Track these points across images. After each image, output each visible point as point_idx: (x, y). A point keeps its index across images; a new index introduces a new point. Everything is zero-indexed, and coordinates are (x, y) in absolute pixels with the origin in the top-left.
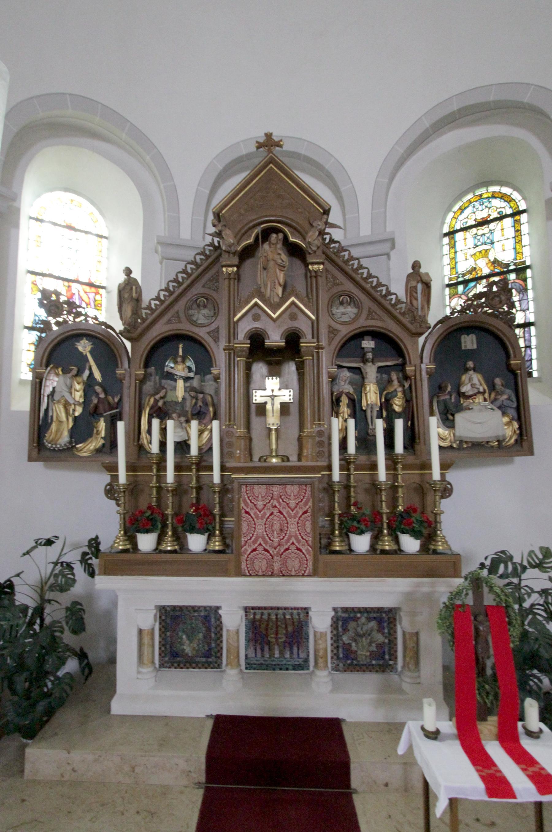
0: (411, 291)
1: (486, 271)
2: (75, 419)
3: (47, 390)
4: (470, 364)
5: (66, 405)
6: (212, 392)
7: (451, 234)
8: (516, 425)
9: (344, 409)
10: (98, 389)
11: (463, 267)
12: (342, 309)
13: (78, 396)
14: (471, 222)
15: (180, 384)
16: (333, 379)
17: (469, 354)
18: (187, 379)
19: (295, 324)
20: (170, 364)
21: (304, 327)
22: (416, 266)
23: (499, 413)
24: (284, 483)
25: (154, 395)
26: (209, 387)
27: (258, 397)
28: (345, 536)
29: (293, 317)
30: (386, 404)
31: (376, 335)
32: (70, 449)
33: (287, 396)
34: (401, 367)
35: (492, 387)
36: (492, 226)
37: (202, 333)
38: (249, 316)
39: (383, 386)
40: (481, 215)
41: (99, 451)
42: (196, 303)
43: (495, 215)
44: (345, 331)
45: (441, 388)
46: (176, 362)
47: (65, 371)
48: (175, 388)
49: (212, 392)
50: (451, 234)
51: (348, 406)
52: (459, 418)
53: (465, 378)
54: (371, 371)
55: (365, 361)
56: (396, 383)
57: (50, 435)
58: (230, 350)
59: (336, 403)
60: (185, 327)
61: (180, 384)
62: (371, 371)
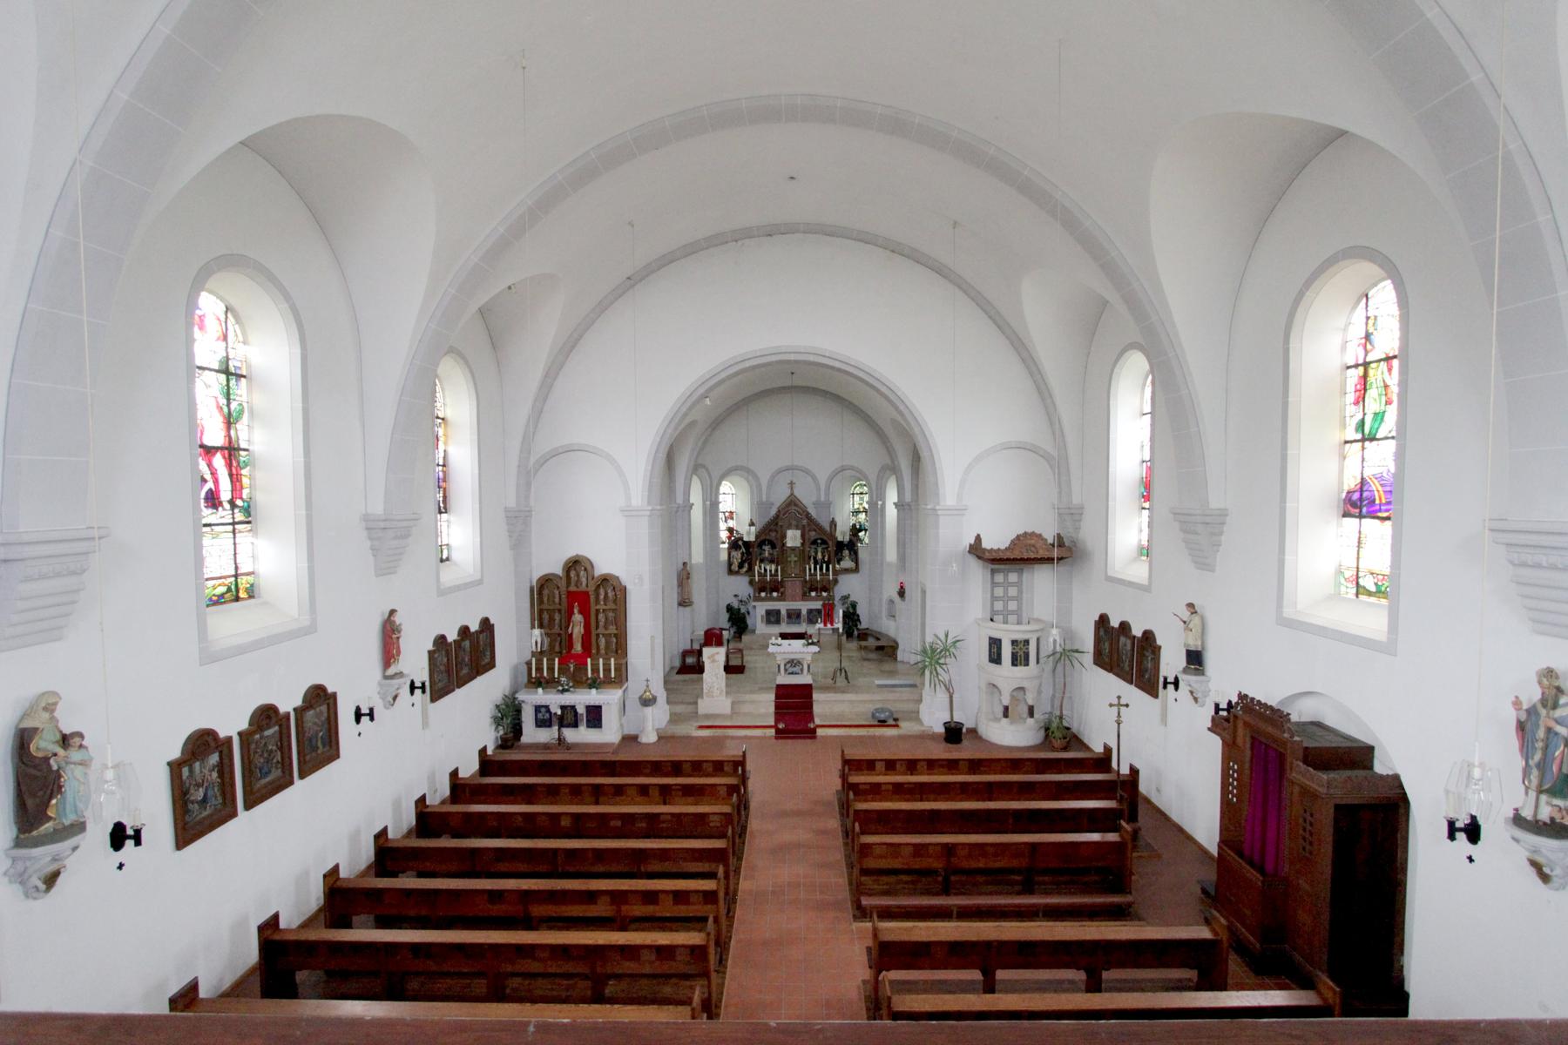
0: (831, 527)
1: (862, 510)
7: (853, 494)
11: (856, 506)
15: (767, 552)
20: (764, 547)
28: (809, 592)
30: (823, 558)
31: (821, 539)
33: (796, 559)
34: (827, 548)
37: (773, 539)
40: (861, 491)
41: (746, 571)
42: (770, 530)
44: (812, 539)
50: (853, 494)
52: (841, 563)
54: (820, 549)
57: (733, 567)
59: (810, 558)
60: (768, 537)
61: (767, 552)
62: (820, 549)
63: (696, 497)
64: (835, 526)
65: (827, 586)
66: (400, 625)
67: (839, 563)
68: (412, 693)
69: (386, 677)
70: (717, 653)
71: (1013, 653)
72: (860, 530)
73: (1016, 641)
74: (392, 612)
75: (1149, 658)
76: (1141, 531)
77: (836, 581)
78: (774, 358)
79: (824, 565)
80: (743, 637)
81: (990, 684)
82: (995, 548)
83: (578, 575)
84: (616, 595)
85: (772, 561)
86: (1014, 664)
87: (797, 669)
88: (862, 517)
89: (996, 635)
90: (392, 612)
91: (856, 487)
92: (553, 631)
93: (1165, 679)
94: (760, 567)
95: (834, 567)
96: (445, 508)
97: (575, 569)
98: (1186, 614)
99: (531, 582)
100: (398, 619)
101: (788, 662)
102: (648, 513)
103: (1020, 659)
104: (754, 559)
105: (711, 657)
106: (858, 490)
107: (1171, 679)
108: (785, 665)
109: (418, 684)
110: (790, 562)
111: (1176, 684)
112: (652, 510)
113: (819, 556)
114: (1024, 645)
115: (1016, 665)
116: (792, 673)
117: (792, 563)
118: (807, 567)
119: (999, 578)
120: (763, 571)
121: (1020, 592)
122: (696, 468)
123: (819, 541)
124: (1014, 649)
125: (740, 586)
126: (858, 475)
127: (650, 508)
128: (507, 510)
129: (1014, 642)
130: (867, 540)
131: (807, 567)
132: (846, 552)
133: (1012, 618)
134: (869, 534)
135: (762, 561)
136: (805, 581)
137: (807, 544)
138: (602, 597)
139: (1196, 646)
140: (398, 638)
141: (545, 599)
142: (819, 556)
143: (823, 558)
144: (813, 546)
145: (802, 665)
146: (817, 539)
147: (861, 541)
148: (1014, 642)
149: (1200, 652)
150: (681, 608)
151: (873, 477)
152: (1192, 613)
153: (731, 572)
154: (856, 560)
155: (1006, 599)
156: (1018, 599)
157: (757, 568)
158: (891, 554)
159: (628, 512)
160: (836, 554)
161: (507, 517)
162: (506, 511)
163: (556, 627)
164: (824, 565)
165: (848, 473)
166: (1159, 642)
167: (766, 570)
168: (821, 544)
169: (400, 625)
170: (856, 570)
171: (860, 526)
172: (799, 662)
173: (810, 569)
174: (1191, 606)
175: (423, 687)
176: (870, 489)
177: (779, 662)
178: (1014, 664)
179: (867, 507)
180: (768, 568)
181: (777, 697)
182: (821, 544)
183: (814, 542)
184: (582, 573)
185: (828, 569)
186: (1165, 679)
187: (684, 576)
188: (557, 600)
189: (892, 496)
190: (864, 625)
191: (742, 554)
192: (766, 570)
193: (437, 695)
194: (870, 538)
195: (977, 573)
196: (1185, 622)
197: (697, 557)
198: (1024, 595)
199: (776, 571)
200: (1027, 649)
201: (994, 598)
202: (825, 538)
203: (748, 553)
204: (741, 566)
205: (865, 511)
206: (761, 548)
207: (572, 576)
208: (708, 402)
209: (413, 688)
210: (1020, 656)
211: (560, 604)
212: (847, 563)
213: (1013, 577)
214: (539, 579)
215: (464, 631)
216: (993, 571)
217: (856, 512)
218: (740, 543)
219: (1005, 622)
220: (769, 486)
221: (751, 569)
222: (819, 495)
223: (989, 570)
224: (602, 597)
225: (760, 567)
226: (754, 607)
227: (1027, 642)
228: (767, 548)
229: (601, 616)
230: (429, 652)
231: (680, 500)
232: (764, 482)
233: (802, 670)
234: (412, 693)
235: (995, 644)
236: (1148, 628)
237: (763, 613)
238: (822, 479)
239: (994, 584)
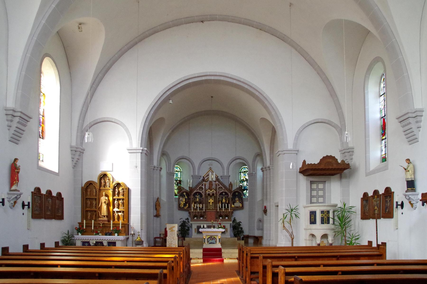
0: (229, 186)
1: (245, 180)
2: (184, 203)
3: (180, 200)
4: (237, 197)
5: (183, 201)
6: (202, 200)
7: (241, 173)
8: (242, 205)
9: (220, 202)
10: (187, 199)
11: (242, 178)
12: (220, 189)
13: (184, 200)
14: (243, 171)
15: (198, 199)
16: (219, 198)
17: (237, 195)
18: (199, 198)
19: (214, 193)
21: (214, 193)
22: (231, 182)
23: (240, 203)
24: (212, 211)
25: (194, 200)
26: (202, 199)
27: (209, 201)
29: (213, 192)
30: (226, 202)
31: (225, 192)
32: (183, 208)
33: (213, 201)
34: (228, 197)
35: (239, 200)
36: (246, 173)
38: (208, 192)
39: (225, 199)
40: (245, 170)
43: (246, 171)
45: (233, 200)
46: (197, 196)
47: (182, 197)
48: (197, 199)
49: (202, 200)
51: (221, 202)
52: (235, 204)
53: (236, 198)
54: (224, 197)
55: (223, 196)
56: (227, 199)
58: (205, 194)
59: (219, 202)
61: (198, 199)
62: (224, 197)
63: (164, 165)
64: (232, 186)
65: (228, 214)
66: (19, 166)
67: (234, 204)
68: (23, 208)
69: (11, 191)
70: (174, 227)
71: (322, 217)
72: (244, 190)
74: (16, 160)
75: (388, 201)
76: (382, 151)
77: (232, 213)
78: (204, 78)
79: (226, 205)
80: (186, 238)
81: (311, 234)
82: (313, 163)
83: (105, 182)
84: (124, 192)
85: (200, 203)
86: (322, 222)
87: (213, 241)
88: (245, 183)
89: (313, 209)
90: (16, 160)
91: (242, 169)
92: (92, 209)
93: (397, 202)
94: (194, 206)
95: (231, 206)
96: (42, 136)
97: (104, 179)
98: (405, 165)
99: (82, 185)
100: (18, 163)
101: (209, 238)
102: (141, 151)
103: (325, 220)
104: (191, 203)
105: (171, 229)
106: (243, 170)
107: (400, 203)
108: (208, 239)
109: (26, 203)
110: (210, 202)
111: (402, 205)
112: (142, 150)
113: (224, 201)
114: (327, 214)
115: (323, 223)
116: (210, 243)
117: (211, 204)
118: (218, 204)
119: (314, 186)
120: (196, 208)
121: (324, 193)
122: (164, 154)
123: (224, 193)
124: (322, 215)
125: (184, 215)
126: (241, 161)
127: (142, 148)
128: (71, 147)
129: (322, 212)
130: (247, 195)
131: (218, 204)
132: (237, 199)
133: (321, 200)
134: (248, 191)
135: (195, 203)
136: (218, 212)
137: (218, 194)
138: (116, 193)
139: (412, 178)
140: (18, 172)
141: (89, 193)
142: (224, 201)
143: (226, 202)
144: (221, 196)
145: (216, 239)
146: (223, 192)
147: (244, 195)
148: (322, 212)
149: (413, 180)
150: (155, 218)
151: (250, 162)
152: (409, 163)
153: (180, 208)
154: (242, 203)
155: (318, 197)
156: (323, 196)
157: (193, 205)
158: (259, 197)
159: (131, 151)
160: (232, 200)
161: (71, 150)
162: (71, 147)
163: (94, 207)
164: (226, 205)
165: (238, 161)
166: (392, 191)
167: (197, 207)
168: (225, 195)
169: (19, 166)
170: (242, 208)
171: (244, 188)
172: (215, 238)
173: (219, 207)
174: (408, 160)
175: (28, 205)
176: (249, 168)
177: (204, 237)
178: (322, 222)
179: (247, 178)
180: (198, 206)
181: (203, 251)
182: (225, 195)
183: (221, 194)
184: (107, 181)
185: (228, 207)
186: (397, 202)
187: (157, 205)
188: (94, 194)
189: (259, 167)
190: (246, 233)
191: (186, 199)
192: (197, 207)
193: (35, 216)
194: (249, 193)
195: (303, 181)
196: (405, 169)
197: (164, 198)
198: (327, 194)
199: (203, 207)
200: (329, 215)
201: (312, 197)
202: (226, 191)
203: (189, 199)
204: (185, 205)
205: (247, 180)
206: (195, 196)
207: (103, 182)
208: (171, 102)
209: (23, 205)
210: (325, 219)
211: (96, 196)
212: (238, 204)
213: (321, 186)
214: (86, 183)
215: (49, 192)
216: (312, 183)
217: (243, 181)
218: (185, 194)
219: (318, 202)
220: (199, 168)
221: (190, 206)
222: (223, 172)
223: (309, 182)
224: (116, 193)
225: (194, 206)
226: (191, 224)
227: (328, 212)
228: (198, 197)
229: (116, 202)
230: (32, 192)
231: (155, 163)
232: (197, 165)
233: (216, 242)
234: (23, 208)
235: (313, 214)
236: (388, 186)
237: (196, 227)
238: (225, 165)
239: (312, 190)
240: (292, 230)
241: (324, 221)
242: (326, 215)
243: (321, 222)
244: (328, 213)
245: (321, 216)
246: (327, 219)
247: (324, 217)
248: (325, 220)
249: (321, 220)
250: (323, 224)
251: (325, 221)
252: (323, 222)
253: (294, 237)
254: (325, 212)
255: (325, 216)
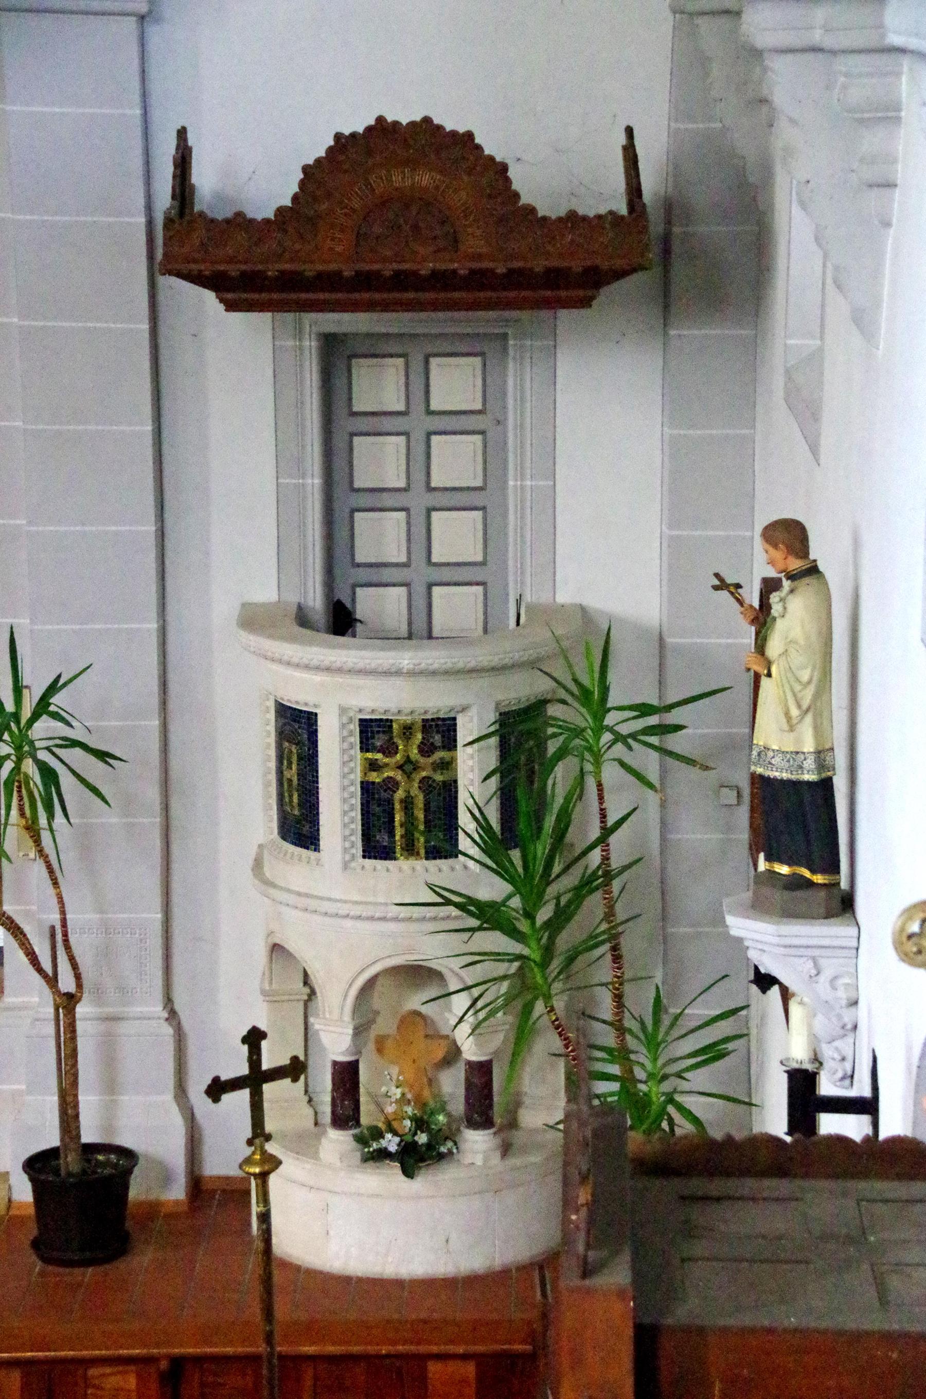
71: (367, 788)
73: (385, 725)
114: (426, 749)
115: (386, 854)
124: (373, 766)
200: (447, 765)
210: (408, 804)
240: (63, 912)
241: (392, 833)
242: (408, 767)
243: (358, 839)
244: (437, 739)
245: (357, 777)
246: (427, 809)
247: (391, 785)
248: (398, 817)
249: (357, 814)
250: (380, 864)
251: (399, 832)
252: (382, 838)
253: (79, 985)
254: (407, 730)
255: (399, 776)
